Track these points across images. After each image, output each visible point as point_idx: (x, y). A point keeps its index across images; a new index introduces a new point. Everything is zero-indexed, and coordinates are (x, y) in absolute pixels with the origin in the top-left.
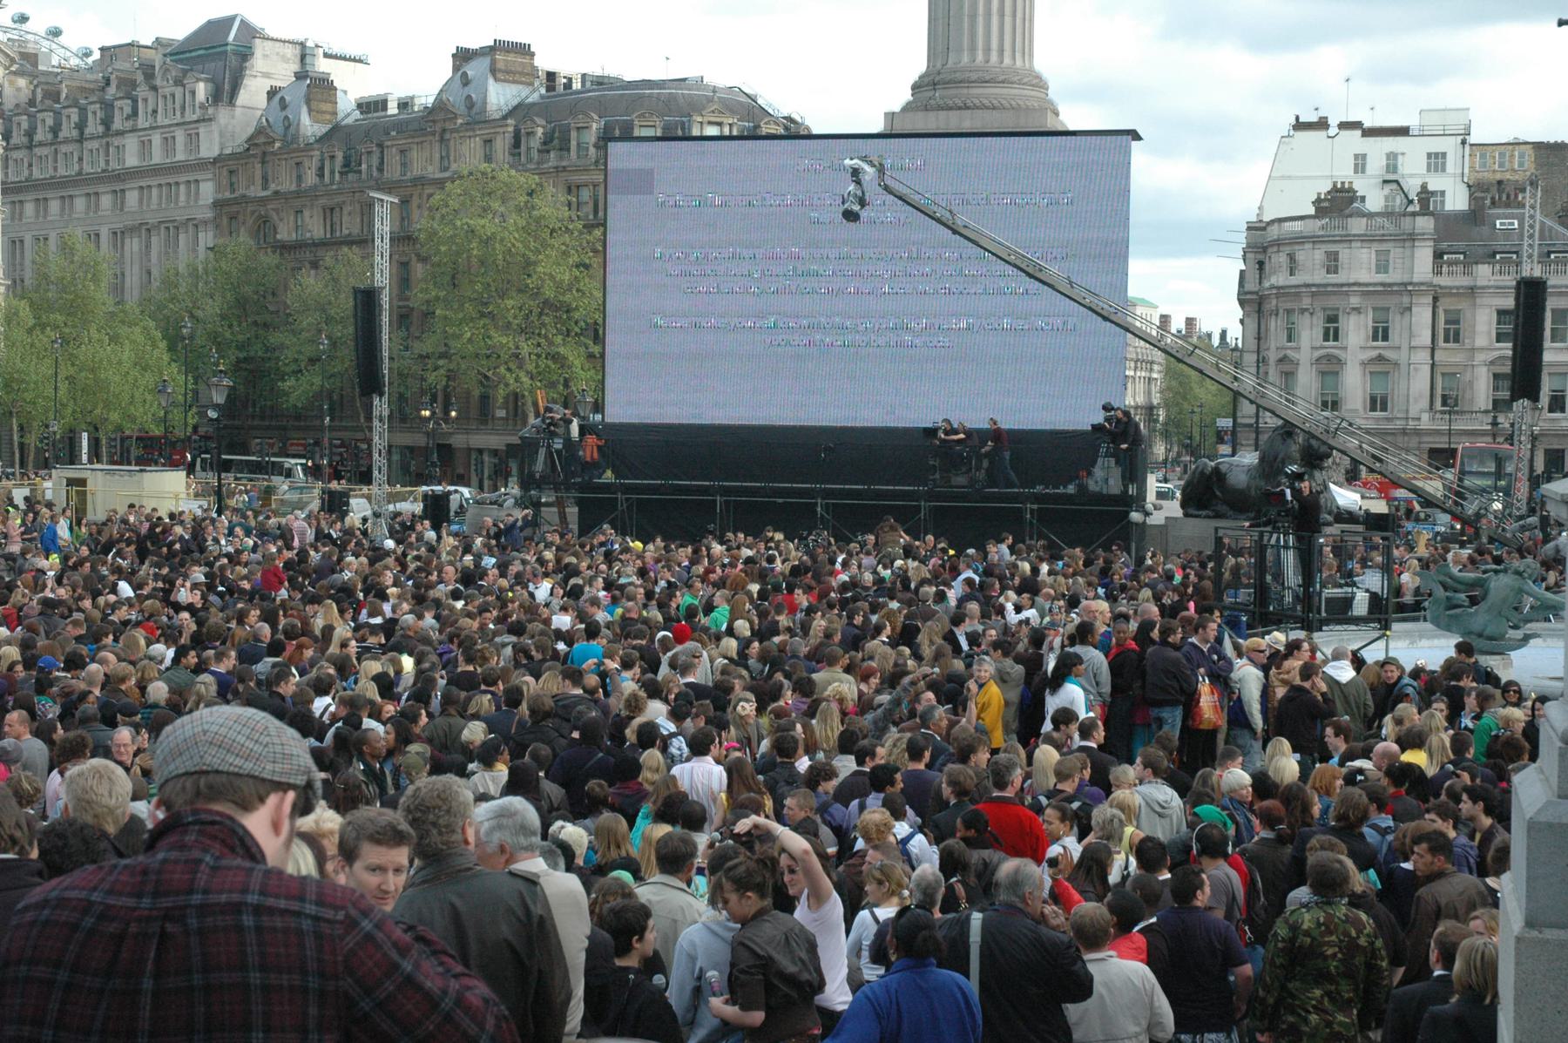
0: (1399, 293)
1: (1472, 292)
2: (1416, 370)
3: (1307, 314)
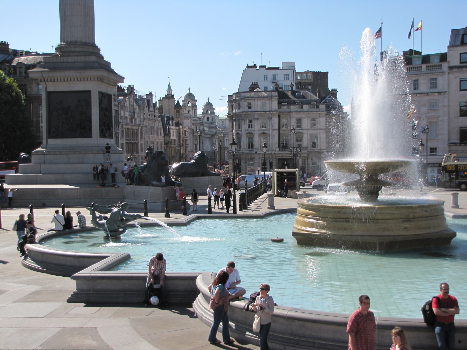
1: (290, 112)
3: (243, 121)
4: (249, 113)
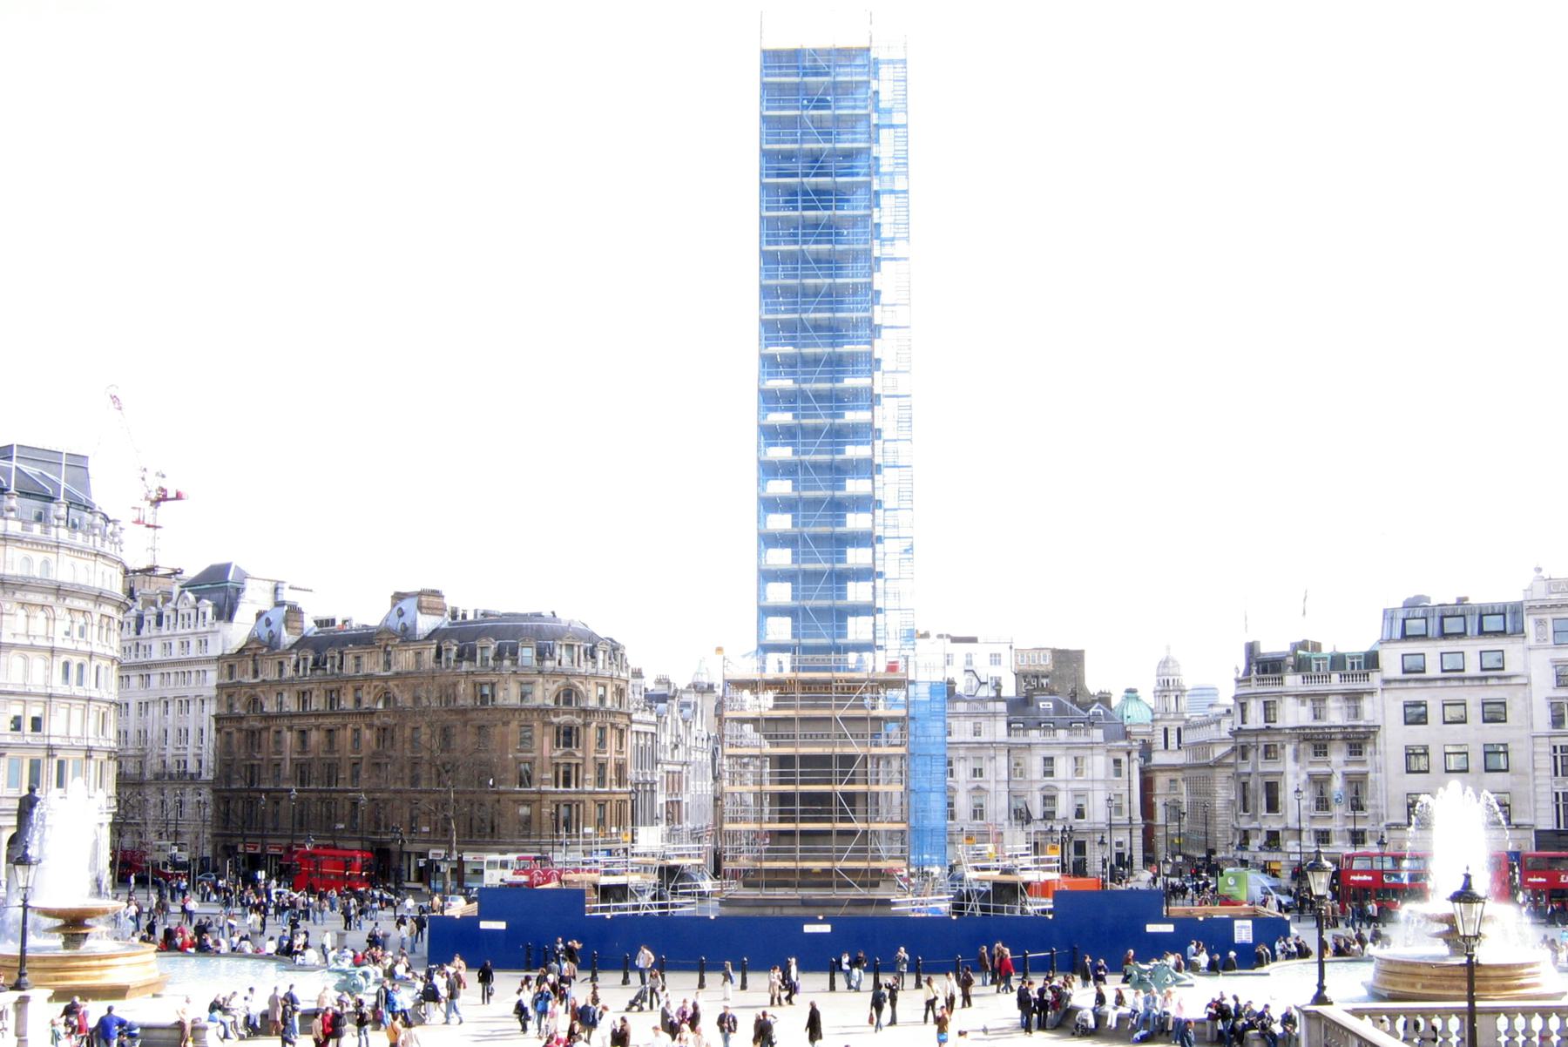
0: (988, 748)
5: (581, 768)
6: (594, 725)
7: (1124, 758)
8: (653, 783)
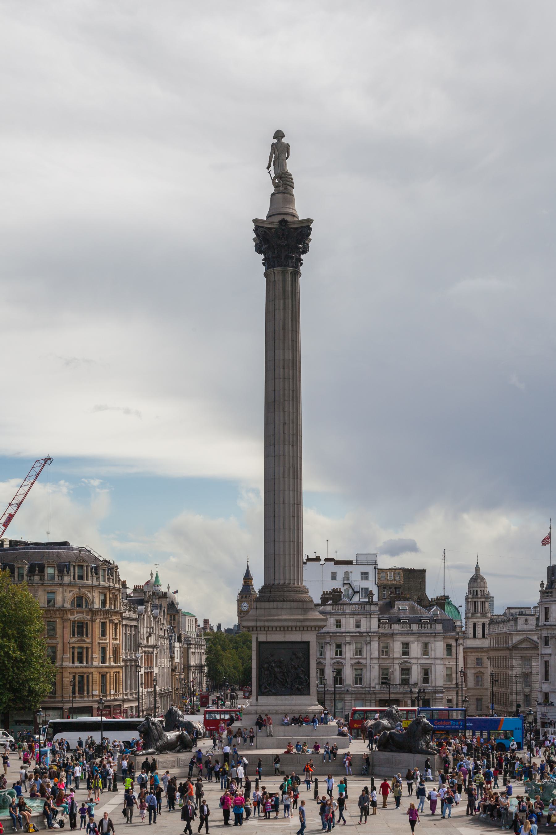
1: (392, 634)
2: (373, 668)
3: (328, 644)
4: (338, 634)
5: (90, 650)
6: (98, 620)
7: (454, 644)
8: (136, 660)
